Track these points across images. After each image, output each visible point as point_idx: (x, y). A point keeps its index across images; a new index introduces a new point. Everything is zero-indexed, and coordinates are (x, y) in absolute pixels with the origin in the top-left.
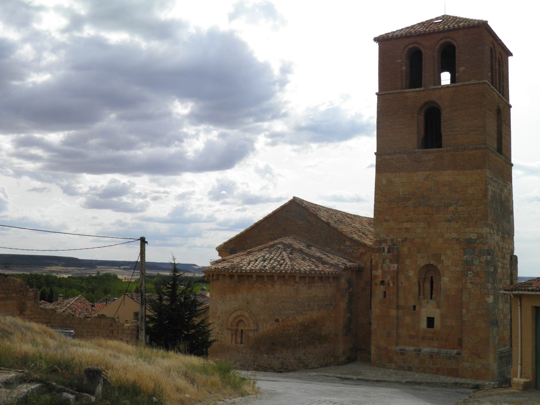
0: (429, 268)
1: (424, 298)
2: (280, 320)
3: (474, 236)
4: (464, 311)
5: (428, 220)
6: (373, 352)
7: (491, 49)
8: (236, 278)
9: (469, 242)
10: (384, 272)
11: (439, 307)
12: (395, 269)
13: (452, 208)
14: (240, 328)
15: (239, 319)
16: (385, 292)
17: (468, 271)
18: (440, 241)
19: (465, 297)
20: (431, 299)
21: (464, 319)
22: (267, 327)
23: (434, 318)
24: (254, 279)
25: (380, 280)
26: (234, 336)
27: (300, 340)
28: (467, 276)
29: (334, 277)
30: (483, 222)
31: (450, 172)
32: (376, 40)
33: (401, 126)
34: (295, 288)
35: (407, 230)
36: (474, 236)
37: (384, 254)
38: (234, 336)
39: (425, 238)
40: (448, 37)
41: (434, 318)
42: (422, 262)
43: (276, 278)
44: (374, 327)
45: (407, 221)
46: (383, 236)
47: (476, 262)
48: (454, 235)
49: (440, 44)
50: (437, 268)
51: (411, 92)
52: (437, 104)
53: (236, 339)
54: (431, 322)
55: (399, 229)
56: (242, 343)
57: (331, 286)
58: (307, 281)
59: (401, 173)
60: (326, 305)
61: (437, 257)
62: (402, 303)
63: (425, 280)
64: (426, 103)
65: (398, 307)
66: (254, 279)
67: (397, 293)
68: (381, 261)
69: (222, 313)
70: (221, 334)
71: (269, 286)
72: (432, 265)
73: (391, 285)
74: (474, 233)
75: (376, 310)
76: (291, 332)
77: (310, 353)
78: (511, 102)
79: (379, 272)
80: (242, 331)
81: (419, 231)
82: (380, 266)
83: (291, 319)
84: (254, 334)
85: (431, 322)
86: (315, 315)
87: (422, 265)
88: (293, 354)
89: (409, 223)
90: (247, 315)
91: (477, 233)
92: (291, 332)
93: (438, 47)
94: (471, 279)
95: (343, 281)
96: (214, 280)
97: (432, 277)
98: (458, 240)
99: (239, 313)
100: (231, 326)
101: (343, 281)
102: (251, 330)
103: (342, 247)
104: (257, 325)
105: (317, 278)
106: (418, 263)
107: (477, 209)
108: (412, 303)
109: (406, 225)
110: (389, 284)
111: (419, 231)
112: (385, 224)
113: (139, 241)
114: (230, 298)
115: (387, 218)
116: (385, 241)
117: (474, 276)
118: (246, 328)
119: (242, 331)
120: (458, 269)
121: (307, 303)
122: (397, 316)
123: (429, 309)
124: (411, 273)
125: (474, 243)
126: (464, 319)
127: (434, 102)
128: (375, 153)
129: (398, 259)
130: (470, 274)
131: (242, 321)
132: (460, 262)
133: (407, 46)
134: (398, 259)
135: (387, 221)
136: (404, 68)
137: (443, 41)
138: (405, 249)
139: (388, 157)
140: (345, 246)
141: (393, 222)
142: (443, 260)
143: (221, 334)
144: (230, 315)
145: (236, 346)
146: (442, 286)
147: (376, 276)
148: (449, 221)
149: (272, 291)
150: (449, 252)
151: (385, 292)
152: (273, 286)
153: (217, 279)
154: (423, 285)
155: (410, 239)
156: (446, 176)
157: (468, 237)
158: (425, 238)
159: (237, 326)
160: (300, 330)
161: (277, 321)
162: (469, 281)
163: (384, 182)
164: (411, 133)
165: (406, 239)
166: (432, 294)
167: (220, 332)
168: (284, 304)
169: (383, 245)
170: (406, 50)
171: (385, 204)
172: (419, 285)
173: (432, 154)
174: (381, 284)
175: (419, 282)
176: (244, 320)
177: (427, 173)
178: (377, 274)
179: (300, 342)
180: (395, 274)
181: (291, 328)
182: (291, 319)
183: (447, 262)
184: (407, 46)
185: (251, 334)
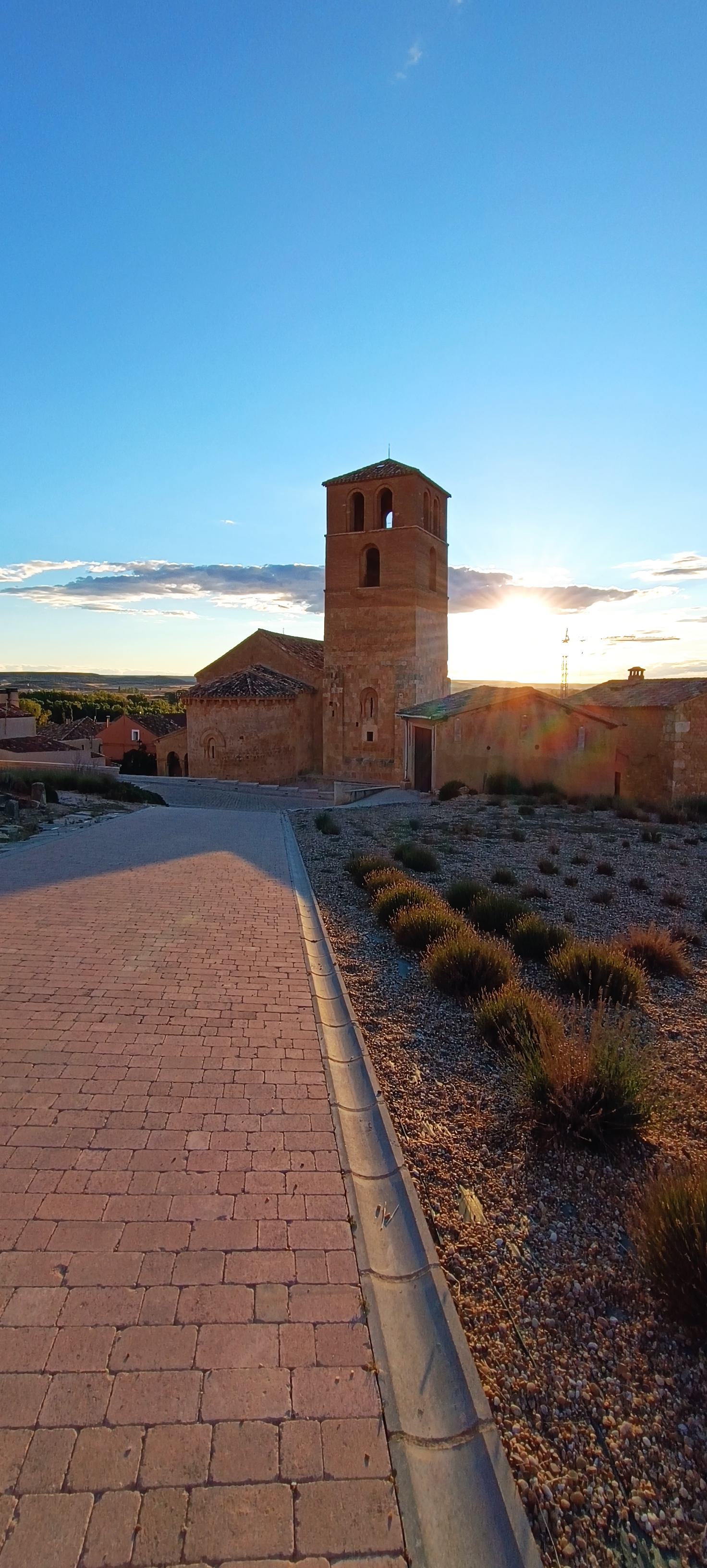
3: (404, 664)
7: (426, 493)
10: (332, 695)
11: (376, 723)
32: (324, 484)
42: (363, 686)
44: (325, 741)
46: (331, 663)
48: (389, 663)
54: (370, 735)
61: (376, 682)
62: (347, 720)
64: (367, 546)
65: (344, 724)
75: (326, 727)
78: (448, 542)
85: (370, 735)
98: (391, 666)
99: (209, 732)
111: (360, 659)
115: (335, 648)
123: (368, 726)
124: (354, 696)
127: (373, 544)
134: (343, 684)
135: (334, 650)
136: (348, 512)
138: (349, 675)
139: (334, 594)
161: (242, 738)
165: (350, 666)
169: (332, 671)
173: (370, 590)
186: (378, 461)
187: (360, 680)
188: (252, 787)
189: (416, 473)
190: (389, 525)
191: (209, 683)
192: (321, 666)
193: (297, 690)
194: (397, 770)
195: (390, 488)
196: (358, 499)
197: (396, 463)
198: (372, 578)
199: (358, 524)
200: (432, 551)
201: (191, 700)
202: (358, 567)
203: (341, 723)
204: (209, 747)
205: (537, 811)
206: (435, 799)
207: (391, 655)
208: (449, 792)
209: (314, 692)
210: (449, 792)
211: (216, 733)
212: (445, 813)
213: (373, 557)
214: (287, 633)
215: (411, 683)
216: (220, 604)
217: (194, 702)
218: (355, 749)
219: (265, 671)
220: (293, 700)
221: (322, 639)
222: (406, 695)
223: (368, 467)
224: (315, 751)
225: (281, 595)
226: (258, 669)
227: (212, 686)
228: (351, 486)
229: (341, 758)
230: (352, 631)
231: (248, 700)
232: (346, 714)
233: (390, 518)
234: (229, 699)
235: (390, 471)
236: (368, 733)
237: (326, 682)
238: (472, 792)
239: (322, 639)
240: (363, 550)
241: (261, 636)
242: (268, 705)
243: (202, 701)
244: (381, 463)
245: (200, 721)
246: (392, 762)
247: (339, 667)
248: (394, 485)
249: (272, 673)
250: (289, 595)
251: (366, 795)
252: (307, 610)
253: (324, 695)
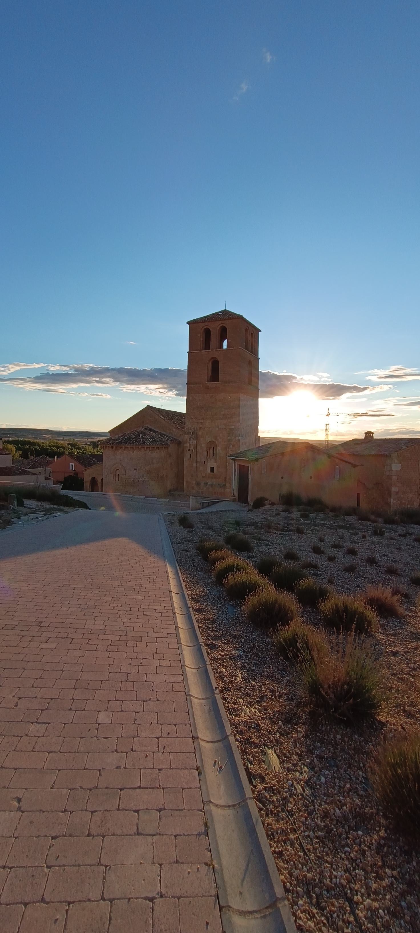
3: (233, 427)
4: (227, 464)
7: (246, 329)
10: (190, 445)
14: (117, 473)
32: (187, 323)
42: (209, 440)
48: (224, 427)
49: (219, 327)
51: (205, 352)
54: (212, 469)
62: (199, 460)
63: (210, 448)
64: (212, 358)
65: (197, 462)
75: (186, 464)
78: (259, 357)
85: (212, 469)
93: (218, 328)
98: (225, 428)
108: (203, 460)
123: (211, 463)
124: (203, 445)
129: (197, 438)
134: (197, 438)
135: (192, 419)
136: (202, 339)
137: (221, 325)
161: (135, 469)
163: (191, 399)
165: (200, 428)
169: (190, 431)
170: (203, 329)
177: (211, 395)
186: (219, 311)
188: (141, 499)
189: (240, 318)
190: (225, 347)
191: (117, 436)
192: (184, 428)
193: (169, 442)
194: (228, 490)
196: (207, 332)
197: (229, 312)
198: (215, 376)
199: (207, 346)
200: (250, 362)
201: (106, 447)
202: (206, 371)
204: (115, 475)
205: (311, 515)
206: (250, 508)
208: (259, 503)
209: (179, 443)
210: (259, 503)
212: (257, 516)
213: (215, 365)
214: (164, 408)
215: (237, 438)
216: (125, 390)
217: (107, 447)
218: (203, 477)
219: (151, 430)
220: (167, 447)
221: (185, 412)
222: (233, 446)
223: (213, 314)
224: (179, 476)
225: (161, 386)
226: (146, 429)
227: (119, 438)
228: (203, 324)
229: (195, 482)
230: (203, 408)
231: (140, 447)
232: (198, 456)
233: (225, 343)
234: (129, 446)
235: (226, 315)
237: (186, 437)
238: (272, 504)
239: (185, 412)
241: (149, 408)
243: (112, 447)
244: (221, 312)
245: (112, 459)
246: (225, 485)
247: (194, 428)
248: (227, 324)
249: (154, 431)
250: (166, 386)
251: (209, 505)
252: (176, 395)
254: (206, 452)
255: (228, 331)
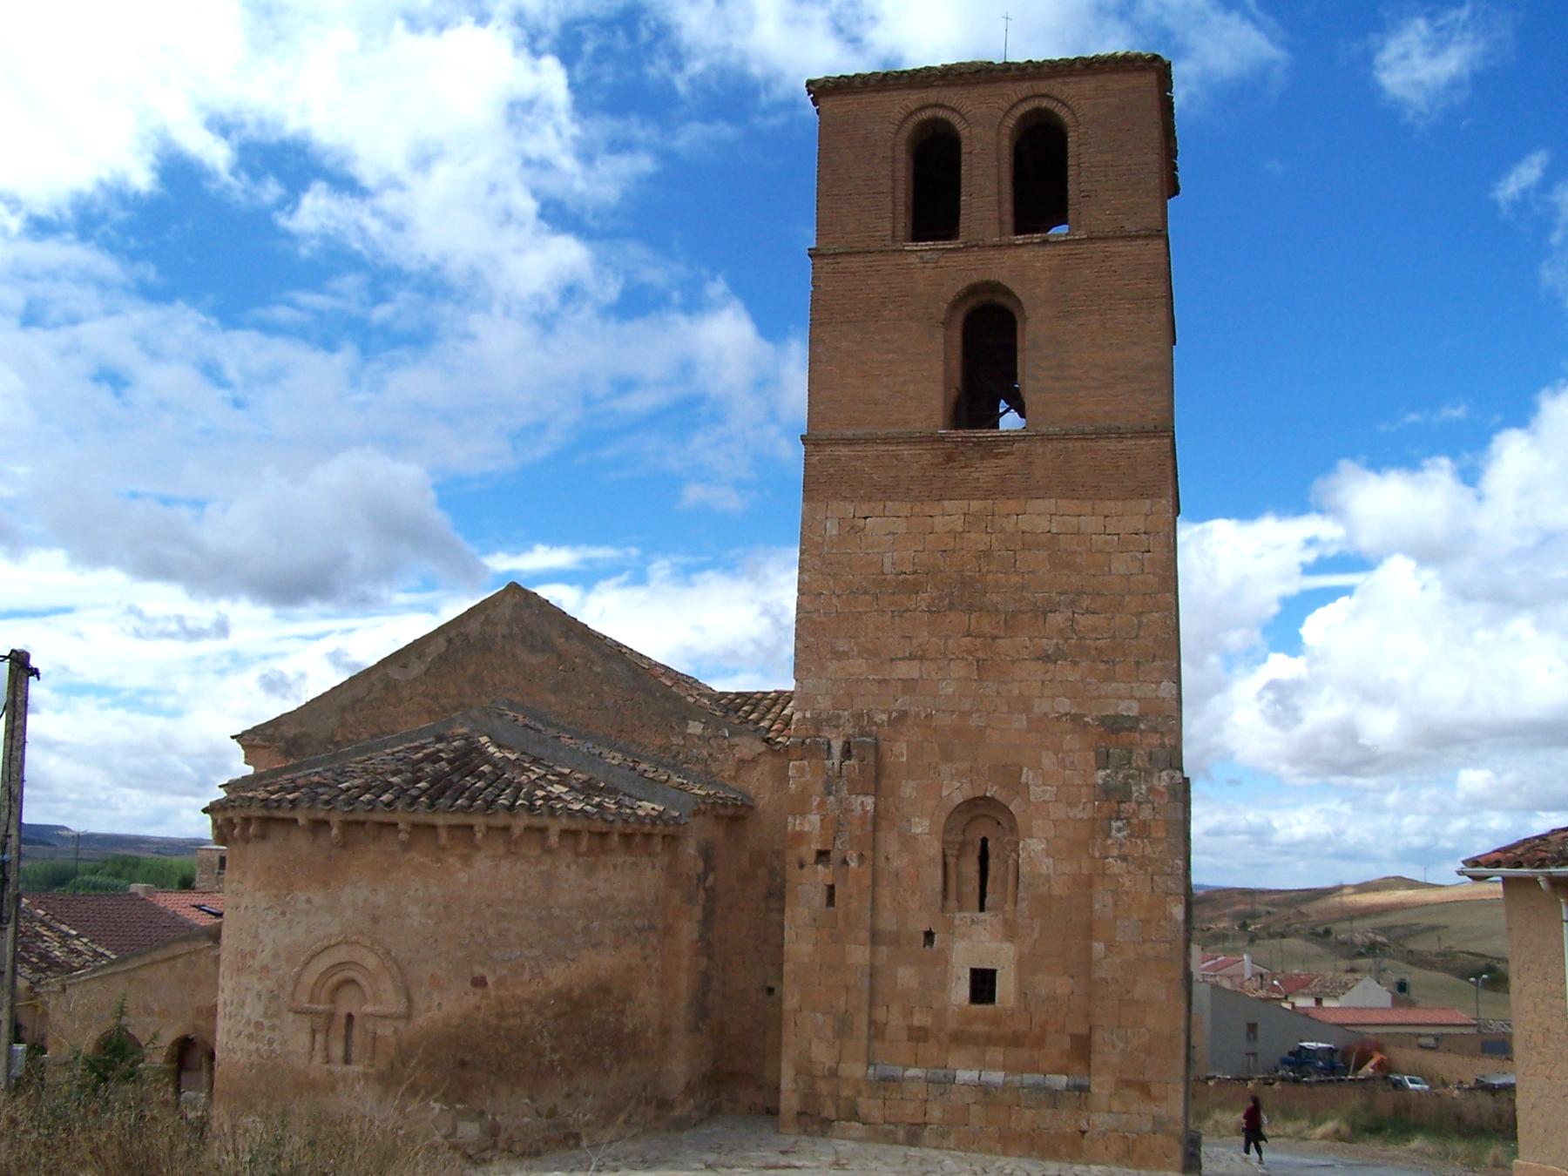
0: (978, 808)
1: (961, 909)
2: (490, 980)
3: (1130, 708)
4: (1099, 947)
5: (980, 655)
6: (787, 1083)
8: (335, 831)
9: (1114, 726)
11: (1010, 932)
12: (870, 808)
13: (1058, 619)
14: (343, 1010)
15: (335, 979)
16: (831, 888)
17: (1110, 819)
18: (1020, 721)
19: (1102, 903)
20: (982, 909)
21: (1099, 973)
22: (444, 1005)
23: (993, 972)
24: (403, 836)
25: (816, 846)
26: (319, 1038)
27: (554, 1050)
28: (1109, 836)
29: (664, 837)
30: (1158, 663)
31: (1049, 504)
33: (891, 356)
34: (544, 868)
35: (909, 685)
36: (1129, 709)
37: (828, 763)
38: (319, 1038)
39: (970, 713)
40: (1044, 96)
41: (993, 972)
42: (956, 792)
43: (479, 835)
45: (911, 658)
47: (1139, 789)
48: (1065, 705)
49: (1018, 112)
50: (1005, 809)
52: (1009, 293)
53: (326, 1048)
54: (983, 984)
55: (880, 682)
56: (347, 1060)
57: (653, 867)
58: (584, 843)
59: (889, 504)
60: (639, 930)
61: (1010, 775)
62: (888, 923)
63: (963, 846)
64: (973, 290)
65: (875, 937)
66: (403, 836)
67: (873, 892)
68: (819, 787)
69: (276, 956)
70: (273, 1028)
71: (451, 860)
72: (992, 799)
73: (853, 864)
74: (1132, 697)
75: (800, 944)
76: (528, 1018)
77: (586, 1094)
79: (812, 823)
80: (350, 1017)
81: (948, 689)
82: (816, 801)
83: (526, 976)
84: (396, 1029)
85: (983, 984)
86: (603, 962)
87: (958, 799)
88: (532, 1099)
89: (916, 663)
90: (371, 961)
91: (1139, 700)
92: (528, 1018)
93: (1010, 122)
94: (1121, 846)
95: (690, 849)
96: (247, 841)
97: (984, 841)
98: (1075, 719)
99: (341, 955)
100: (310, 1002)
101: (690, 849)
102: (384, 1017)
103: (675, 740)
104: (409, 999)
105: (616, 838)
106: (945, 793)
107: (1140, 623)
109: (905, 670)
110: (845, 862)
112: (833, 666)
113: (7, 663)
114: (309, 901)
115: (842, 645)
116: (833, 721)
117: (1130, 835)
118: (368, 1008)
119: (350, 1017)
120: (1077, 813)
121: (581, 923)
122: (872, 966)
123: (978, 942)
124: (920, 827)
125: (1131, 729)
126: (1099, 973)
128: (803, 438)
129: (876, 778)
130: (1119, 830)
131: (351, 982)
132: (1084, 790)
133: (911, 114)
135: (839, 655)
137: (1027, 107)
138: (900, 751)
139: (845, 451)
140: (685, 737)
141: (861, 661)
142: (1027, 785)
143: (273, 1028)
144: (307, 963)
145: (330, 1073)
146: (1024, 869)
147: (800, 837)
148: (1047, 658)
149: (463, 877)
150: (1048, 760)
151: (831, 888)
152: (467, 860)
153: (263, 836)
154: (957, 865)
155: (918, 714)
156: (1040, 516)
157: (1110, 712)
158: (970, 713)
159: (333, 1001)
160: (558, 1016)
161: (479, 982)
162: (1115, 852)
163: (832, 528)
164: (925, 376)
165: (903, 715)
166: (983, 895)
167: (266, 1023)
168: (504, 924)
170: (910, 125)
171: (835, 601)
172: (945, 865)
174: (817, 862)
175: (945, 856)
176: (360, 978)
177: (976, 505)
178: (807, 828)
179: (556, 1057)
180: (869, 828)
181: (525, 1008)
182: (526, 976)
183: (1038, 792)
184: (911, 114)
185: (386, 1030)
187: (946, 768)
195: (1063, 113)
203: (864, 935)
207: (1073, 675)
211: (371, 961)
228: (913, 98)
230: (916, 589)
232: (885, 895)
234: (440, 820)
236: (975, 973)
240: (954, 306)
242: (590, 852)
253: (795, 824)
254: (940, 873)
255: (1072, 138)
